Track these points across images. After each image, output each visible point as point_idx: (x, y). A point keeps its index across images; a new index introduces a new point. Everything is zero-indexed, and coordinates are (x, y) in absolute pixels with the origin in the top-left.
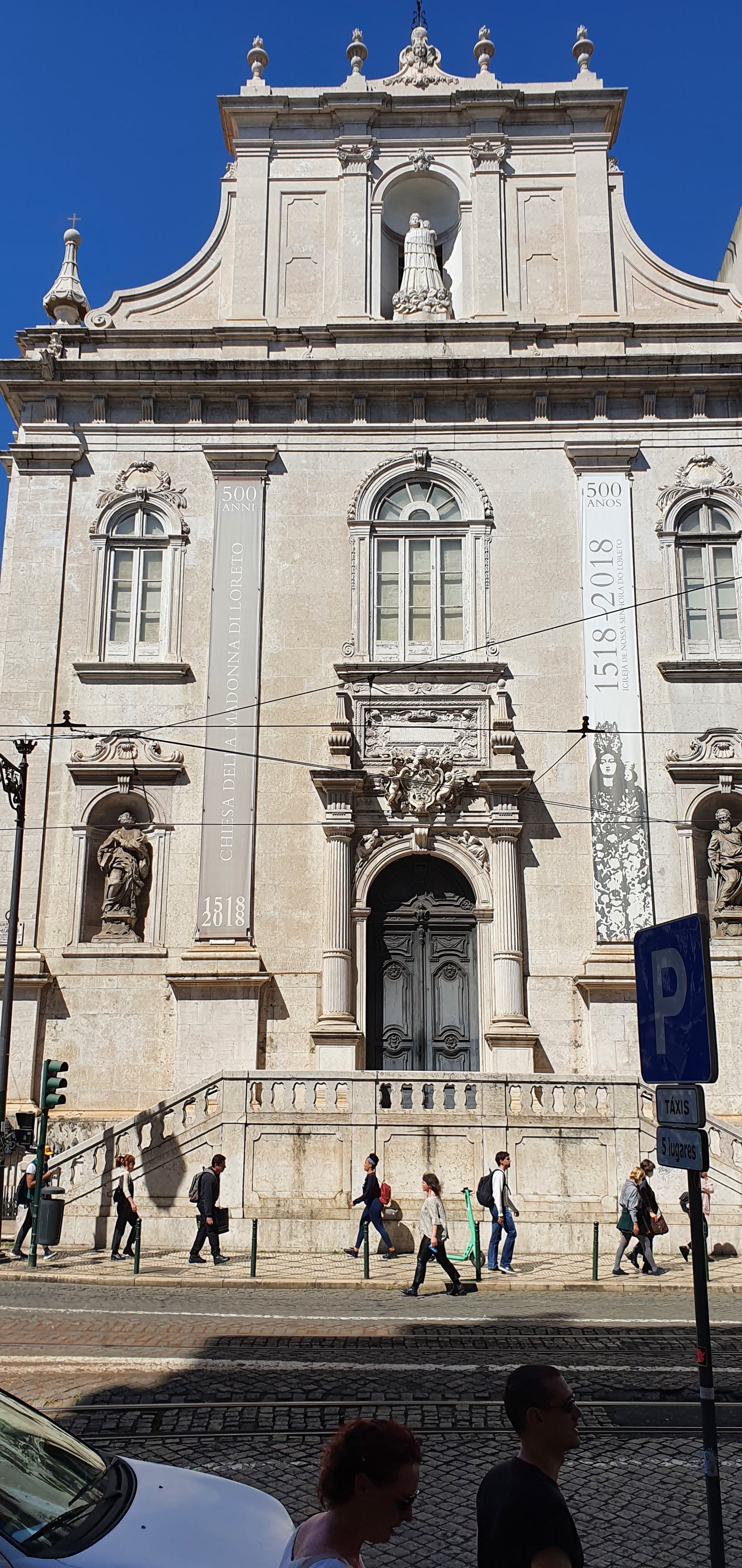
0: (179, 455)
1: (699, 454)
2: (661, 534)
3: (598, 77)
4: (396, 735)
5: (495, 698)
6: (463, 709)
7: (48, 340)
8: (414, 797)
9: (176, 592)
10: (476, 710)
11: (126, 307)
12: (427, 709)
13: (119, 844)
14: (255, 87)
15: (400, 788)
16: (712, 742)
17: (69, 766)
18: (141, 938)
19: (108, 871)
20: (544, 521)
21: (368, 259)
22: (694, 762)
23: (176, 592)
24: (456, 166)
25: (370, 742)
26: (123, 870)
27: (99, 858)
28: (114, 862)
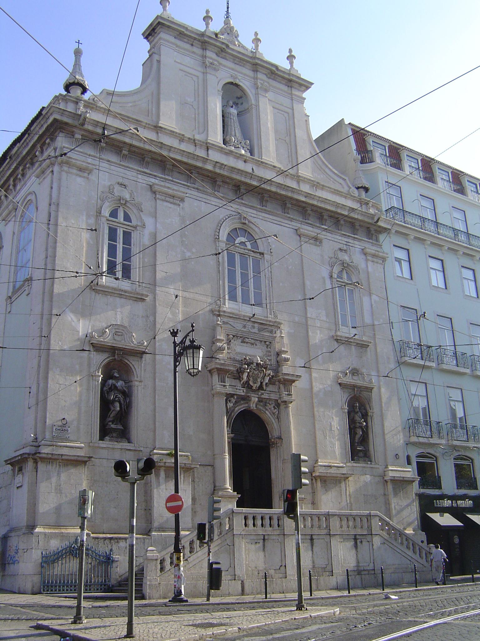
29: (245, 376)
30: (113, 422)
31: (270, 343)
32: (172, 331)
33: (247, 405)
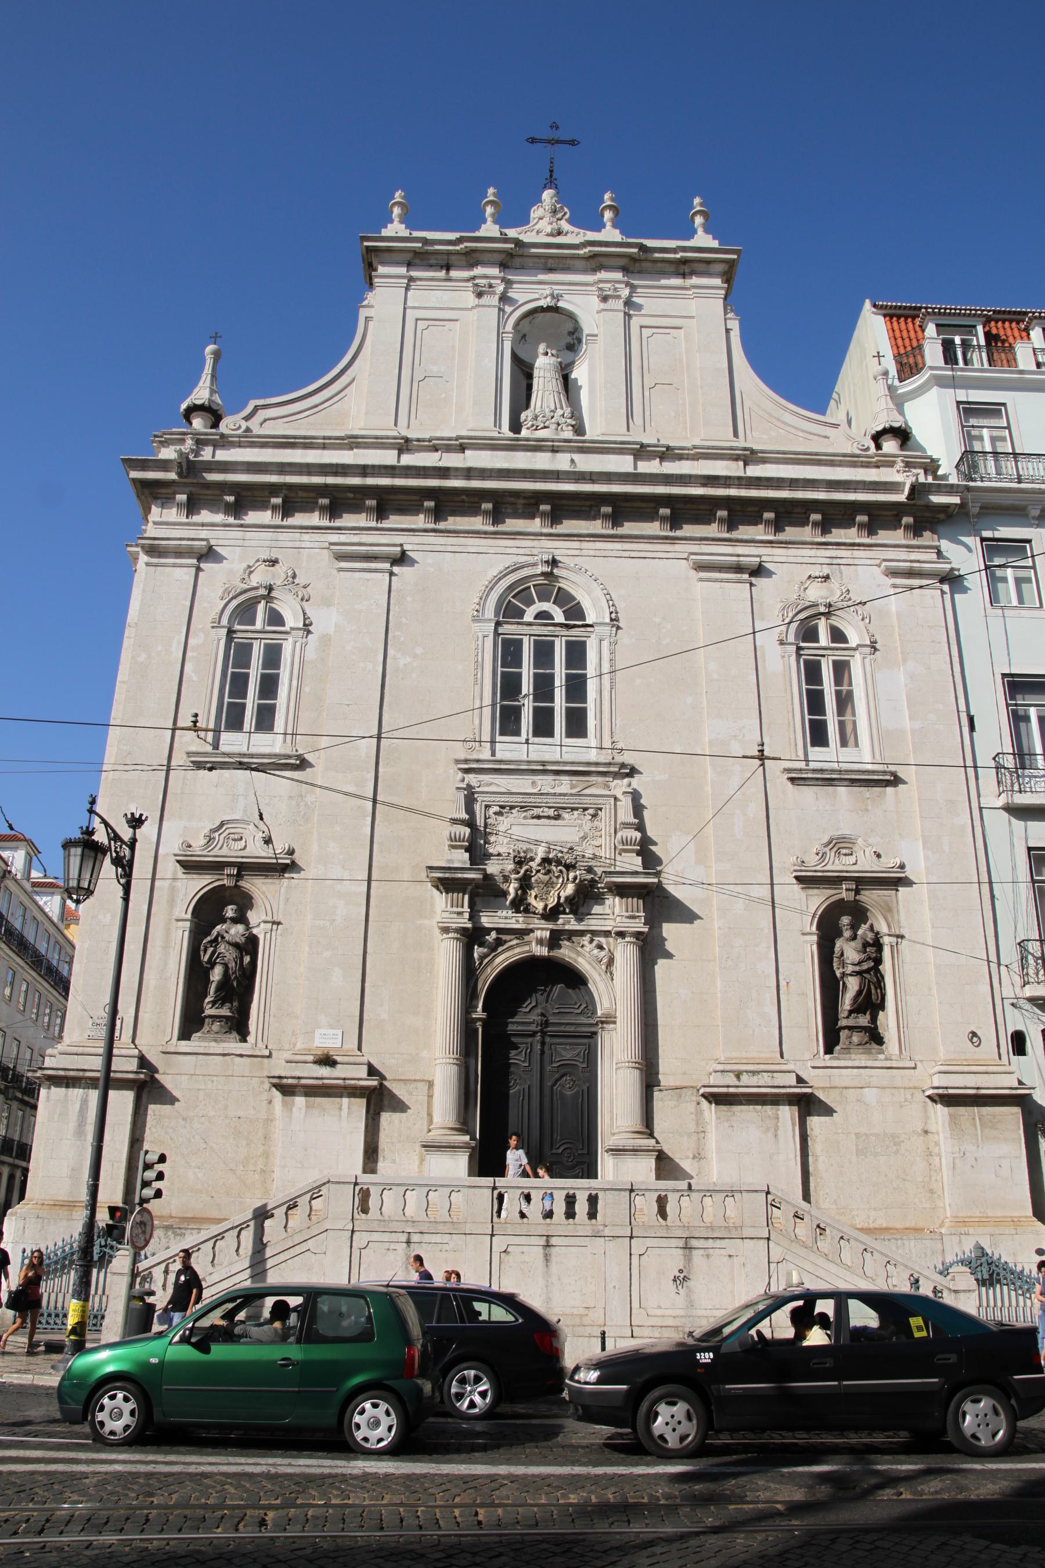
0: (305, 550)
1: (816, 571)
2: (782, 643)
3: (714, 238)
5: (620, 796)
7: (182, 441)
8: (536, 897)
9: (295, 683)
10: (601, 809)
11: (262, 414)
12: (550, 807)
13: (223, 937)
14: (395, 228)
15: (521, 887)
16: (835, 849)
17: (175, 855)
18: (244, 1040)
19: (212, 964)
20: (669, 626)
21: (499, 381)
22: (818, 868)
23: (295, 683)
24: (584, 299)
26: (226, 966)
27: (202, 953)
28: (217, 957)
31: (601, 809)
33: (527, 948)
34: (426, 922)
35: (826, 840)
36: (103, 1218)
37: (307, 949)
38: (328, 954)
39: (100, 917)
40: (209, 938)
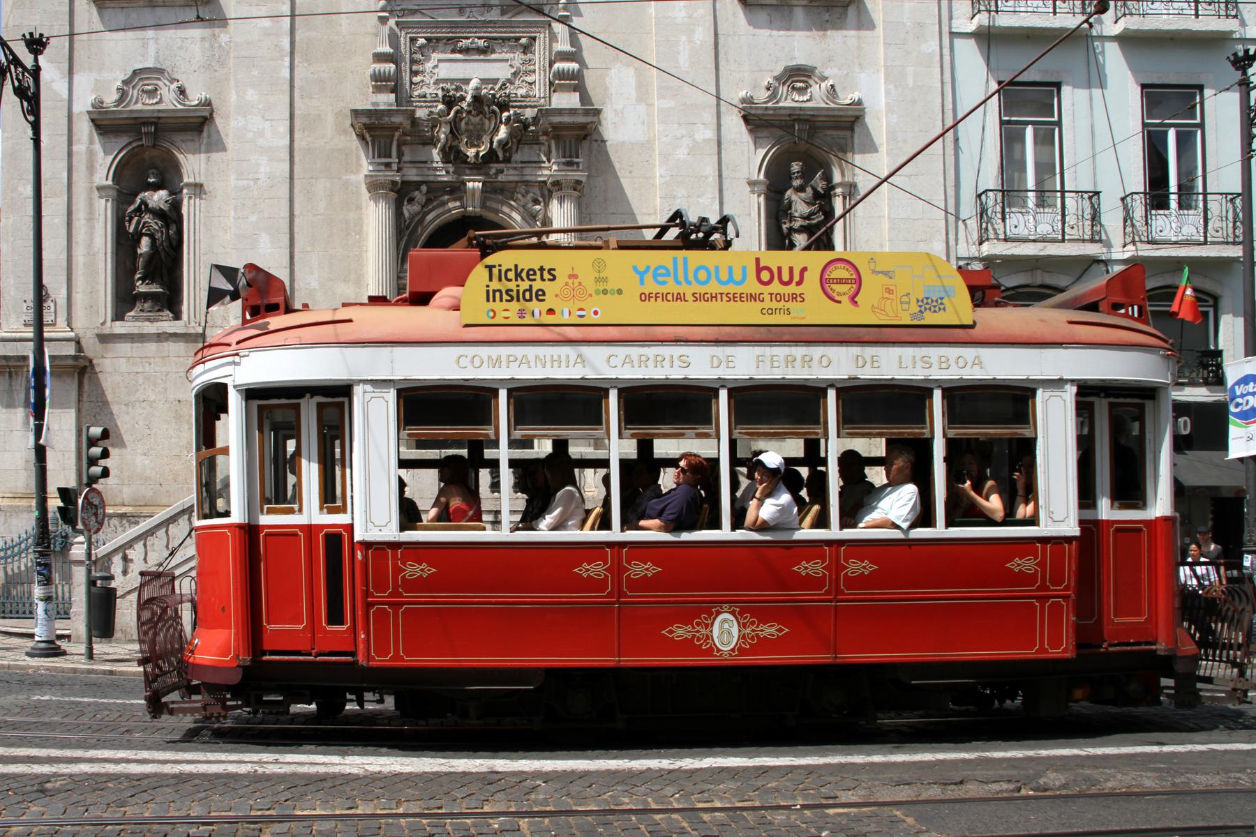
4: (445, 71)
6: (519, 38)
12: (479, 38)
13: (147, 205)
22: (769, 105)
25: (416, 80)
26: (152, 236)
29: (442, 134)
30: (143, 279)
32: (28, 37)
34: (353, 177)
35: (779, 70)
36: (54, 503)
37: (232, 214)
38: (253, 218)
39: (21, 189)
40: (132, 208)
